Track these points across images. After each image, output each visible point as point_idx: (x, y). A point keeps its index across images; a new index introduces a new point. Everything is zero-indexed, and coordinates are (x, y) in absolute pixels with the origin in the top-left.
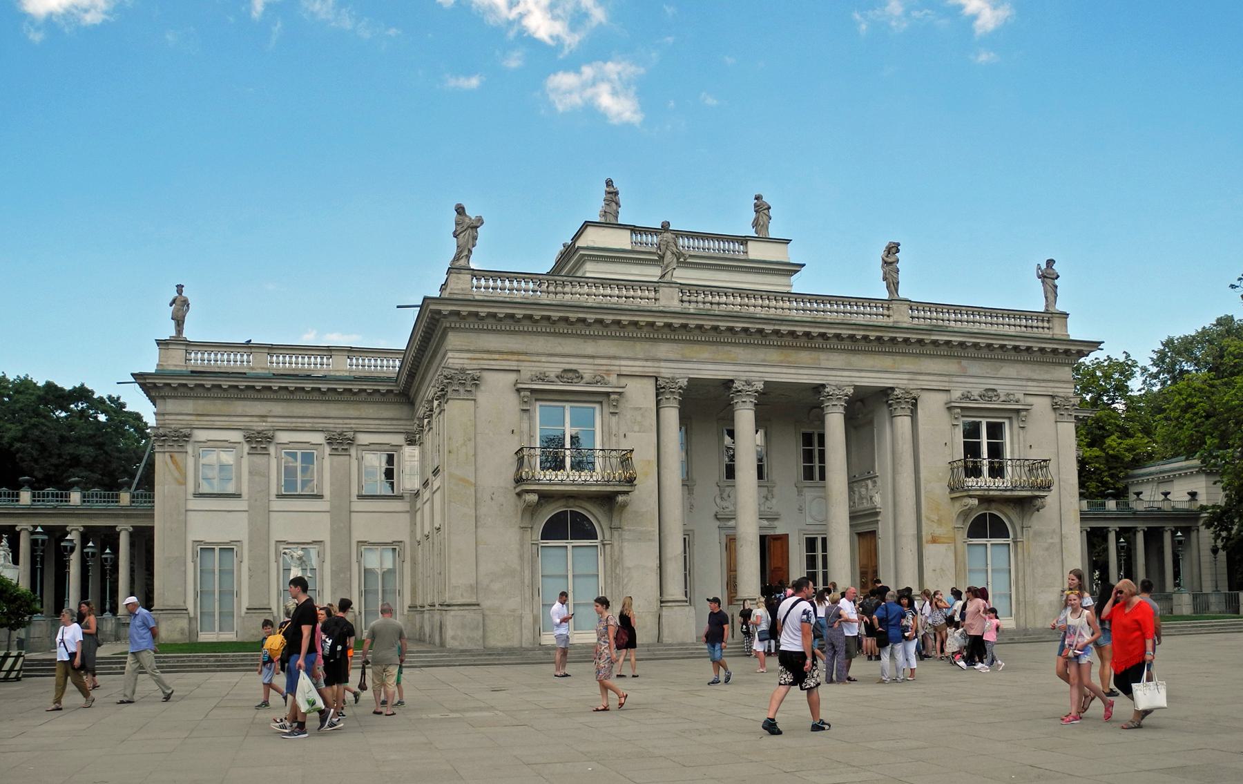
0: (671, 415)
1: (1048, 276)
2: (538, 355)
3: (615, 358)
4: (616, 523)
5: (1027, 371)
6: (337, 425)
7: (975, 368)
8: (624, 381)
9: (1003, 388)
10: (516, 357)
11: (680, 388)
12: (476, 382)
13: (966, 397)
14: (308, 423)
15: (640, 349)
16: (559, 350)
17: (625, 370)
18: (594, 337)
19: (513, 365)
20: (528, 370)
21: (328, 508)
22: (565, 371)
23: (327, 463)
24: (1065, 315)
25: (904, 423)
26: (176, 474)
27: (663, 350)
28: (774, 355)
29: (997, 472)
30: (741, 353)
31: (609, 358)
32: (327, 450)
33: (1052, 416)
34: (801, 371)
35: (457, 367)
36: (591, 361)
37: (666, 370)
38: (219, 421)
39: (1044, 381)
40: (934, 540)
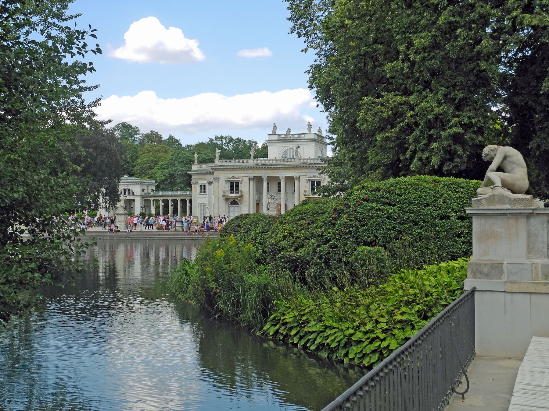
0: (251, 183)
12: (219, 179)
15: (246, 172)
20: (227, 177)
27: (250, 172)
28: (270, 171)
30: (264, 171)
38: (203, 180)
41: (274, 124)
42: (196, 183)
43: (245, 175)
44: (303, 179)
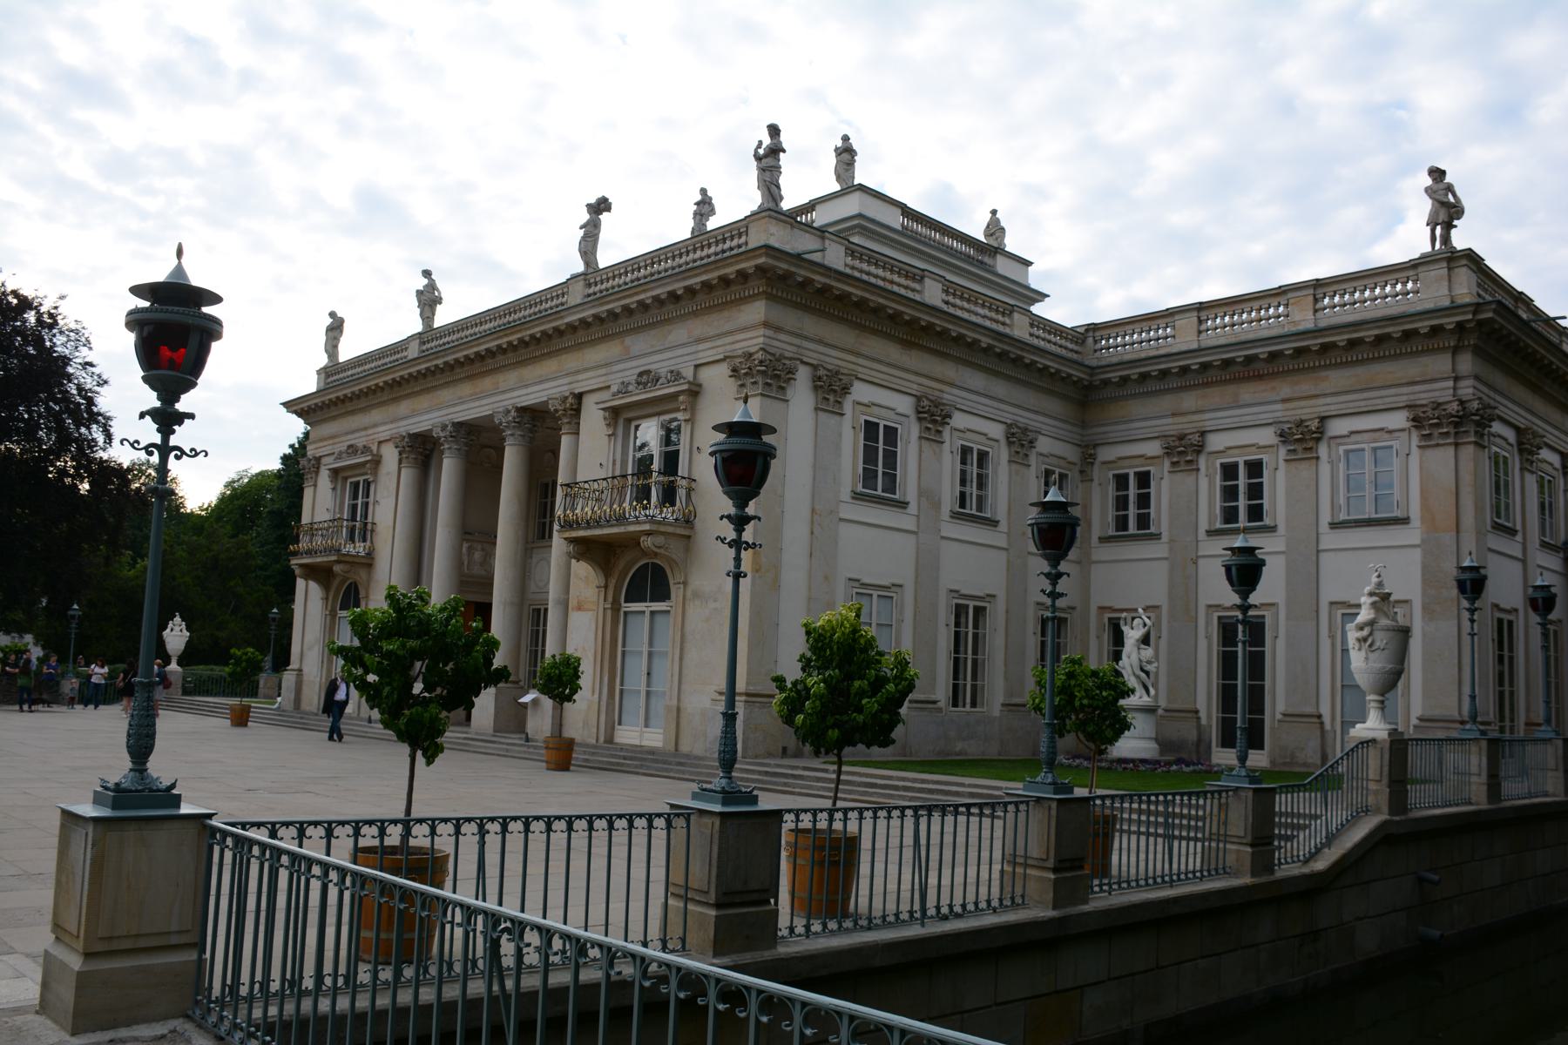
5: (698, 327)
9: (661, 364)
30: (446, 395)
39: (720, 336)
41: (703, 191)
43: (384, 432)
44: (593, 418)
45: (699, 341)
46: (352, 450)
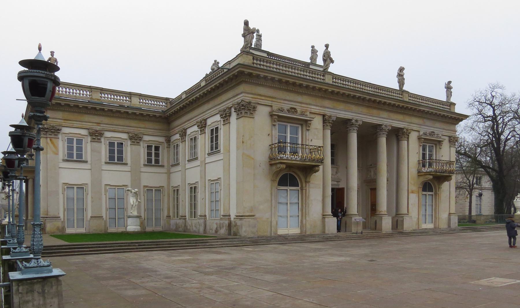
1: (448, 87)
2: (280, 99)
3: (310, 104)
4: (308, 180)
6: (136, 131)
7: (428, 123)
8: (313, 116)
10: (271, 99)
11: (333, 121)
13: (425, 134)
14: (120, 128)
15: (319, 101)
16: (288, 98)
17: (313, 111)
18: (302, 94)
19: (269, 103)
21: (129, 170)
22: (292, 108)
23: (129, 148)
24: (454, 104)
25: (404, 143)
26: (54, 149)
27: (327, 103)
28: (364, 110)
29: (430, 165)
30: (354, 108)
31: (307, 104)
32: (129, 142)
33: (449, 144)
34: (374, 118)
35: (247, 101)
36: (300, 105)
37: (328, 112)
38: (76, 124)
40: (412, 192)
42: (56, 131)
45: (444, 129)
46: (293, 110)
